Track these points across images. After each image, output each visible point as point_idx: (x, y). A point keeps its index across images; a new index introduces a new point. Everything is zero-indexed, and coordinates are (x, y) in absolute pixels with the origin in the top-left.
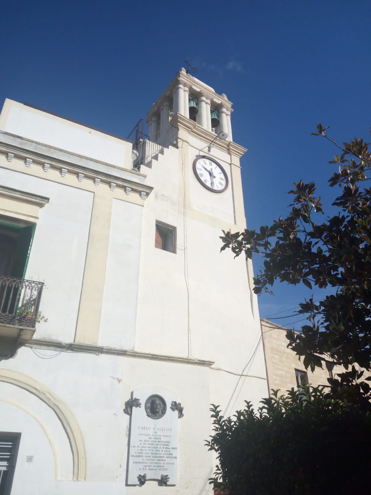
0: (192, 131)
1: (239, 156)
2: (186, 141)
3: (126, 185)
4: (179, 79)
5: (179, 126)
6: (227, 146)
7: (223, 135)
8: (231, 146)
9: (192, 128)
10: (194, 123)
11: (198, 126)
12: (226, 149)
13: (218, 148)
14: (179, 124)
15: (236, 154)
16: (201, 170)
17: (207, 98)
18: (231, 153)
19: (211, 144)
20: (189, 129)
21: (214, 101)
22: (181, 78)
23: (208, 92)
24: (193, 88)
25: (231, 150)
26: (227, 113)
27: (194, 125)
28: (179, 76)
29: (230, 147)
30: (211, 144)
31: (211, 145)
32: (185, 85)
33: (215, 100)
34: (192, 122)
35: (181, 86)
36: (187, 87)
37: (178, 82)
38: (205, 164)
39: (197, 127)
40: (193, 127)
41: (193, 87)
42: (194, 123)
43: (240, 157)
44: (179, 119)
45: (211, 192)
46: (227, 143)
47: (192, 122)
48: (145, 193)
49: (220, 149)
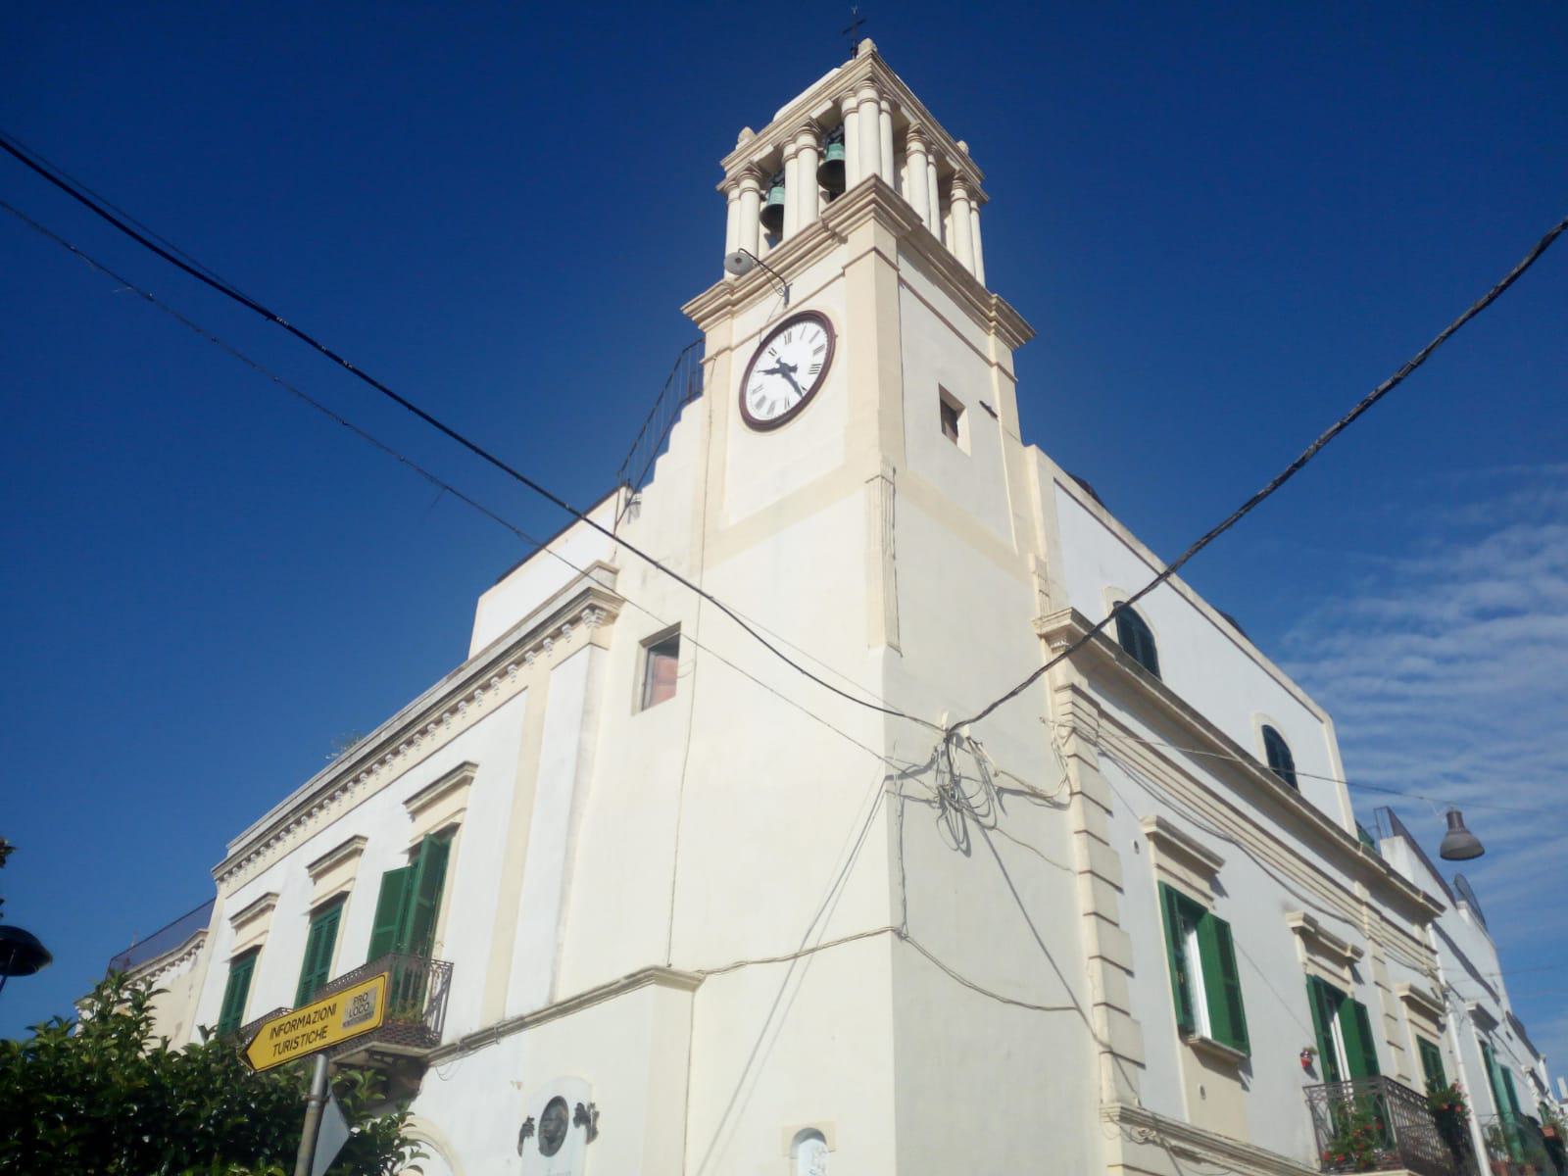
0: (734, 305)
1: (866, 214)
2: (718, 354)
3: (558, 625)
4: (719, 187)
5: (705, 330)
6: (826, 231)
7: (738, 260)
8: (832, 220)
9: (729, 299)
10: (722, 284)
11: (736, 280)
12: (830, 241)
13: (810, 264)
14: (701, 326)
15: (859, 219)
16: (760, 387)
17: (794, 140)
18: (844, 235)
19: (783, 280)
20: (725, 307)
21: (820, 117)
22: (728, 176)
23: (796, 116)
24: (761, 160)
25: (837, 230)
26: (855, 105)
27: (725, 290)
28: (722, 175)
29: (831, 225)
30: (783, 280)
31: (786, 281)
32: (737, 181)
33: (815, 114)
34: (718, 290)
35: (734, 194)
36: (744, 179)
37: (723, 197)
38: (773, 353)
39: (737, 284)
40: (728, 295)
41: (756, 158)
42: (722, 284)
43: (872, 214)
44: (694, 318)
45: (788, 425)
46: (820, 224)
47: (718, 290)
48: (587, 611)
49: (818, 258)
